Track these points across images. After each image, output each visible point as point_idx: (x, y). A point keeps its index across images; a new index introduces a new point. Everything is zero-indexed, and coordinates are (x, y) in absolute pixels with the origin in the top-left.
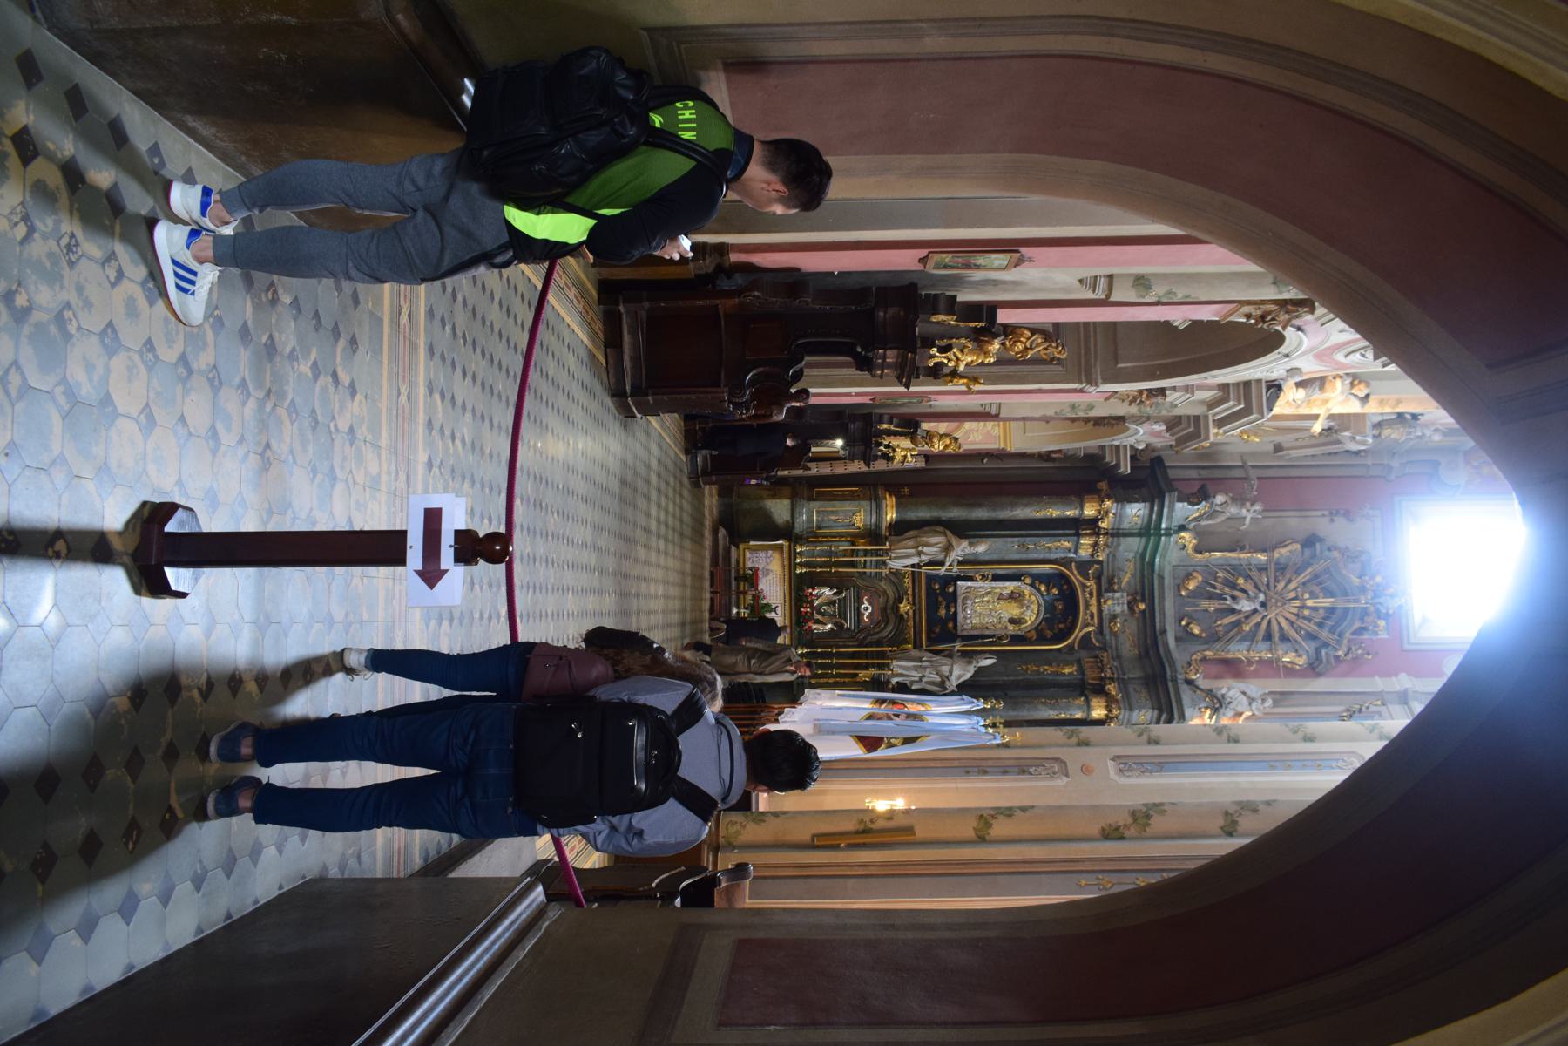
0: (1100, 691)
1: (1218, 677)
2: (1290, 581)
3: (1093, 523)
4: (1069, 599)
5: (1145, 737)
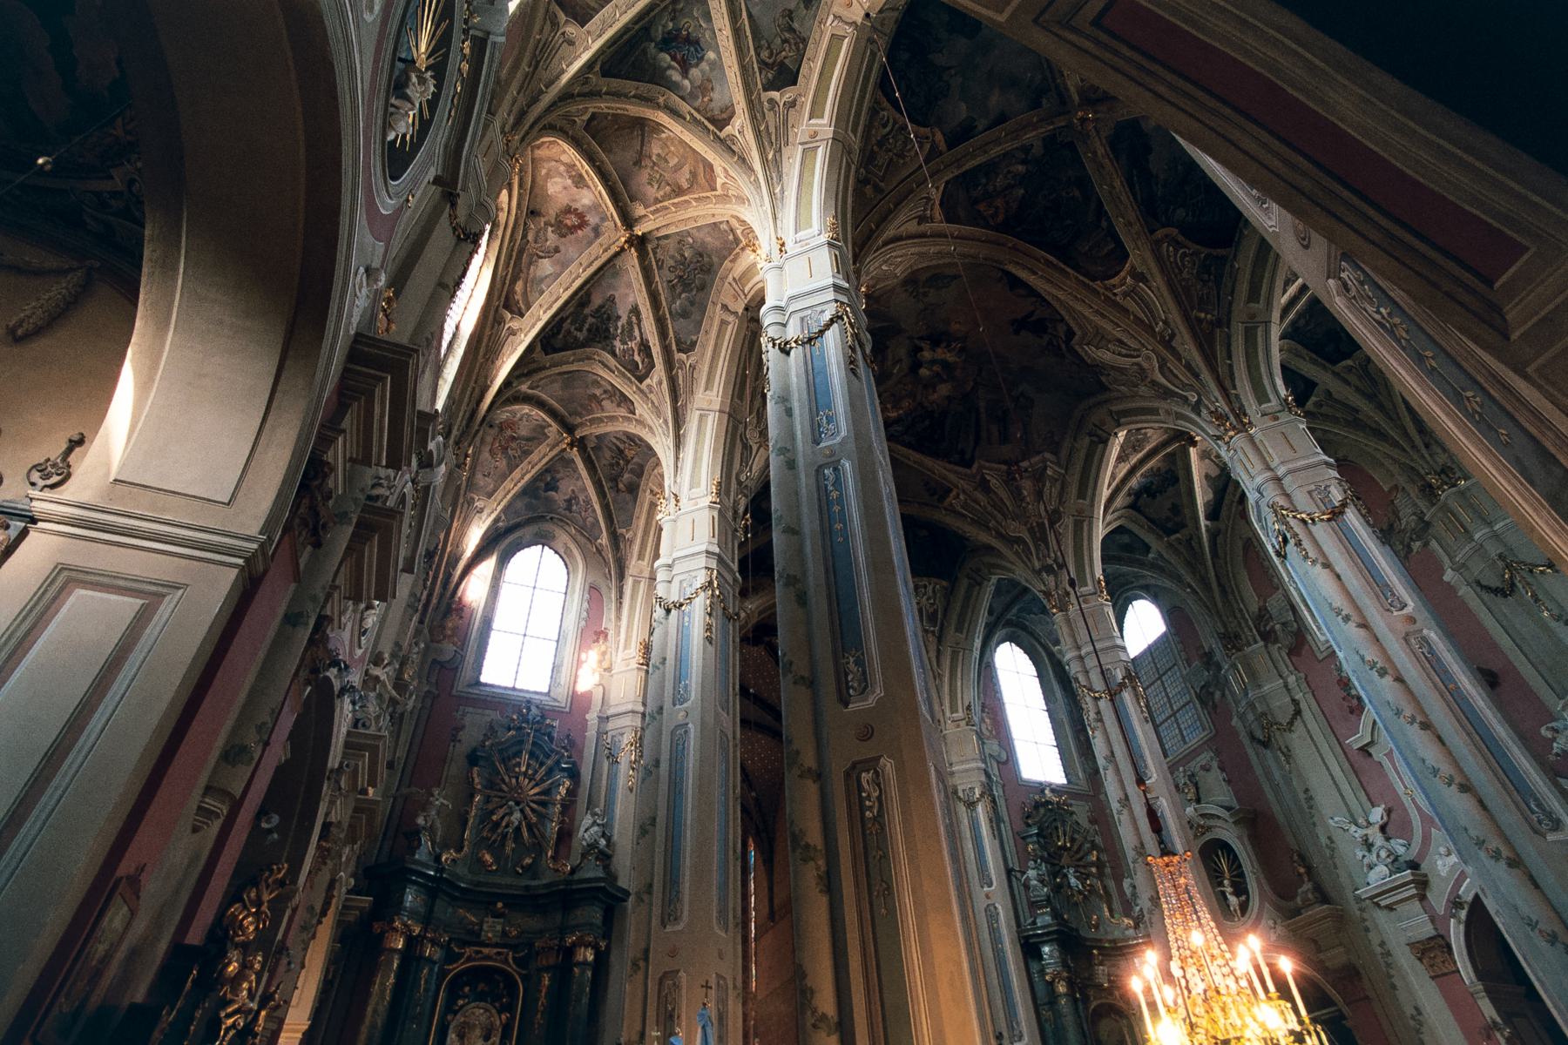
0: (569, 952)
1: (570, 848)
2: (503, 780)
3: (411, 941)
4: (477, 975)
5: (645, 897)
